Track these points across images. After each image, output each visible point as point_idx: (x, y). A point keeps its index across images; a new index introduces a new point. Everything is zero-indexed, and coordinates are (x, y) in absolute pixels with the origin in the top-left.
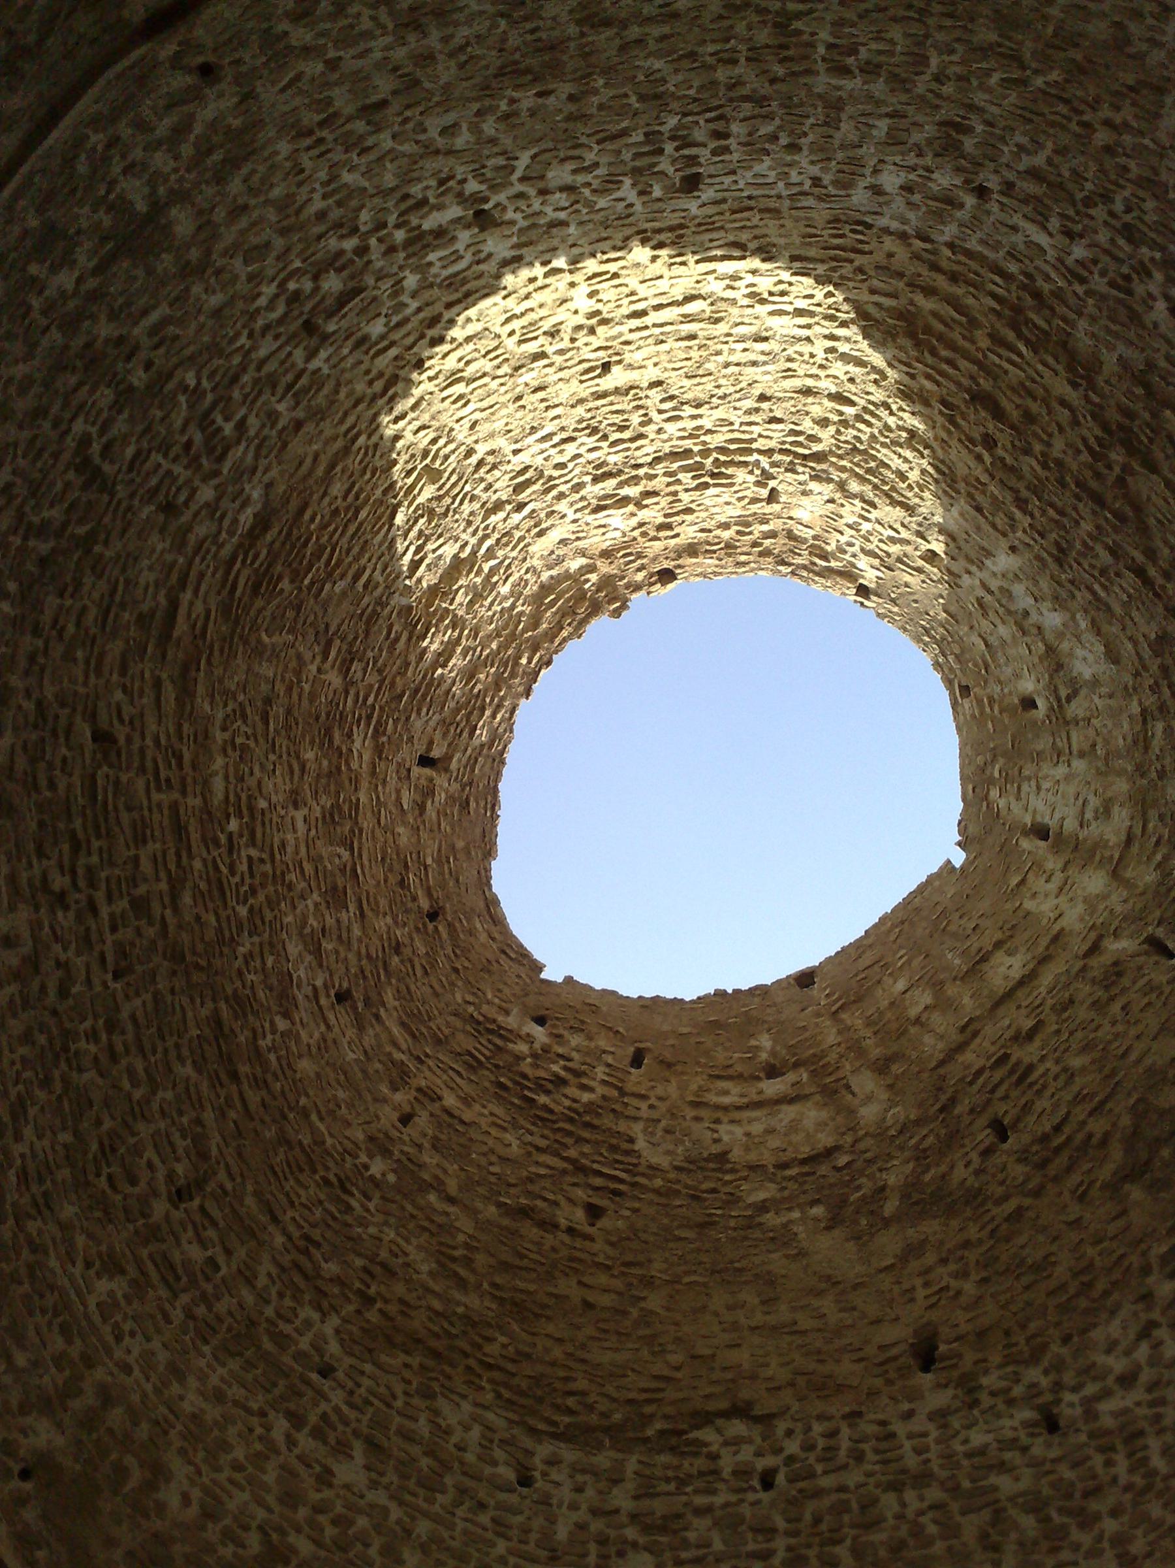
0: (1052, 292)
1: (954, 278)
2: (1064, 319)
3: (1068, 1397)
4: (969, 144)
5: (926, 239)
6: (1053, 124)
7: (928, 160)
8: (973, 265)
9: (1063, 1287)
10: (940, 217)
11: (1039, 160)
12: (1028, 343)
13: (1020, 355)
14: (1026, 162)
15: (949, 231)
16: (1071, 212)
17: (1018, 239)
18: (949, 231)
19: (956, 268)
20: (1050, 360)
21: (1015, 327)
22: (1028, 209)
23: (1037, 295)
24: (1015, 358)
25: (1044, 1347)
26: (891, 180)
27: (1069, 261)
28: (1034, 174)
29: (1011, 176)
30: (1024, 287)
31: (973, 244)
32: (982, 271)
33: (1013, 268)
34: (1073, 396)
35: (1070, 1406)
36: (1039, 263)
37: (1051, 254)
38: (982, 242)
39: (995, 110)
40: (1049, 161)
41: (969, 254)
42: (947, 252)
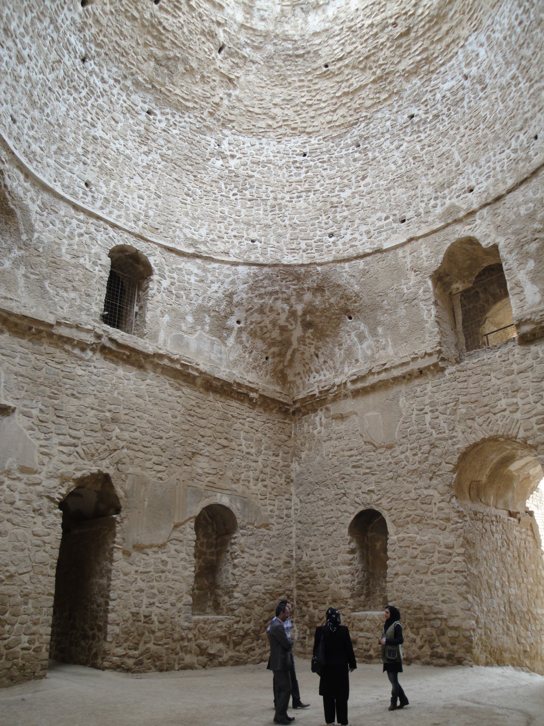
0: (431, 78)
1: (448, 46)
2: (422, 78)
3: (92, 62)
4: (479, 87)
5: (463, 46)
6: (471, 117)
7: (480, 70)
8: (449, 56)
9: (119, 46)
10: (466, 57)
11: (465, 103)
12: (420, 61)
13: (418, 55)
14: (467, 100)
15: (461, 56)
16: (448, 101)
17: (449, 78)
18: (461, 56)
19: (450, 49)
20: (412, 66)
21: (427, 58)
22: (455, 89)
23: (432, 72)
24: (417, 53)
25: (102, 47)
26: (482, 52)
27: (437, 91)
28: (462, 99)
29: (466, 91)
30: (436, 69)
31: (453, 61)
32: (446, 58)
33: (442, 69)
34: (401, 67)
35: (90, 65)
36: (440, 79)
37: (441, 86)
38: (453, 65)
39: (482, 104)
40: (463, 107)
41: (452, 57)
42: (455, 50)
